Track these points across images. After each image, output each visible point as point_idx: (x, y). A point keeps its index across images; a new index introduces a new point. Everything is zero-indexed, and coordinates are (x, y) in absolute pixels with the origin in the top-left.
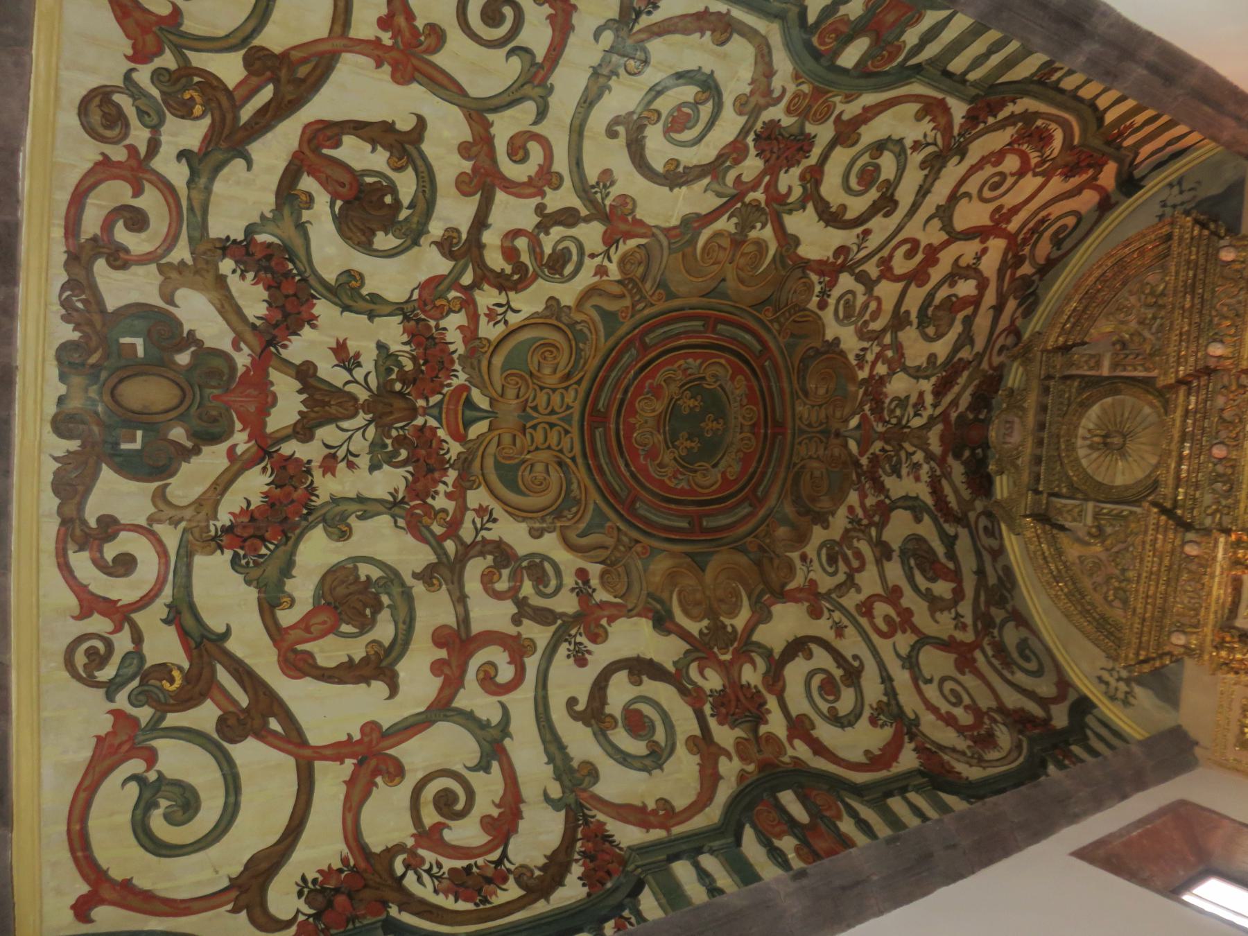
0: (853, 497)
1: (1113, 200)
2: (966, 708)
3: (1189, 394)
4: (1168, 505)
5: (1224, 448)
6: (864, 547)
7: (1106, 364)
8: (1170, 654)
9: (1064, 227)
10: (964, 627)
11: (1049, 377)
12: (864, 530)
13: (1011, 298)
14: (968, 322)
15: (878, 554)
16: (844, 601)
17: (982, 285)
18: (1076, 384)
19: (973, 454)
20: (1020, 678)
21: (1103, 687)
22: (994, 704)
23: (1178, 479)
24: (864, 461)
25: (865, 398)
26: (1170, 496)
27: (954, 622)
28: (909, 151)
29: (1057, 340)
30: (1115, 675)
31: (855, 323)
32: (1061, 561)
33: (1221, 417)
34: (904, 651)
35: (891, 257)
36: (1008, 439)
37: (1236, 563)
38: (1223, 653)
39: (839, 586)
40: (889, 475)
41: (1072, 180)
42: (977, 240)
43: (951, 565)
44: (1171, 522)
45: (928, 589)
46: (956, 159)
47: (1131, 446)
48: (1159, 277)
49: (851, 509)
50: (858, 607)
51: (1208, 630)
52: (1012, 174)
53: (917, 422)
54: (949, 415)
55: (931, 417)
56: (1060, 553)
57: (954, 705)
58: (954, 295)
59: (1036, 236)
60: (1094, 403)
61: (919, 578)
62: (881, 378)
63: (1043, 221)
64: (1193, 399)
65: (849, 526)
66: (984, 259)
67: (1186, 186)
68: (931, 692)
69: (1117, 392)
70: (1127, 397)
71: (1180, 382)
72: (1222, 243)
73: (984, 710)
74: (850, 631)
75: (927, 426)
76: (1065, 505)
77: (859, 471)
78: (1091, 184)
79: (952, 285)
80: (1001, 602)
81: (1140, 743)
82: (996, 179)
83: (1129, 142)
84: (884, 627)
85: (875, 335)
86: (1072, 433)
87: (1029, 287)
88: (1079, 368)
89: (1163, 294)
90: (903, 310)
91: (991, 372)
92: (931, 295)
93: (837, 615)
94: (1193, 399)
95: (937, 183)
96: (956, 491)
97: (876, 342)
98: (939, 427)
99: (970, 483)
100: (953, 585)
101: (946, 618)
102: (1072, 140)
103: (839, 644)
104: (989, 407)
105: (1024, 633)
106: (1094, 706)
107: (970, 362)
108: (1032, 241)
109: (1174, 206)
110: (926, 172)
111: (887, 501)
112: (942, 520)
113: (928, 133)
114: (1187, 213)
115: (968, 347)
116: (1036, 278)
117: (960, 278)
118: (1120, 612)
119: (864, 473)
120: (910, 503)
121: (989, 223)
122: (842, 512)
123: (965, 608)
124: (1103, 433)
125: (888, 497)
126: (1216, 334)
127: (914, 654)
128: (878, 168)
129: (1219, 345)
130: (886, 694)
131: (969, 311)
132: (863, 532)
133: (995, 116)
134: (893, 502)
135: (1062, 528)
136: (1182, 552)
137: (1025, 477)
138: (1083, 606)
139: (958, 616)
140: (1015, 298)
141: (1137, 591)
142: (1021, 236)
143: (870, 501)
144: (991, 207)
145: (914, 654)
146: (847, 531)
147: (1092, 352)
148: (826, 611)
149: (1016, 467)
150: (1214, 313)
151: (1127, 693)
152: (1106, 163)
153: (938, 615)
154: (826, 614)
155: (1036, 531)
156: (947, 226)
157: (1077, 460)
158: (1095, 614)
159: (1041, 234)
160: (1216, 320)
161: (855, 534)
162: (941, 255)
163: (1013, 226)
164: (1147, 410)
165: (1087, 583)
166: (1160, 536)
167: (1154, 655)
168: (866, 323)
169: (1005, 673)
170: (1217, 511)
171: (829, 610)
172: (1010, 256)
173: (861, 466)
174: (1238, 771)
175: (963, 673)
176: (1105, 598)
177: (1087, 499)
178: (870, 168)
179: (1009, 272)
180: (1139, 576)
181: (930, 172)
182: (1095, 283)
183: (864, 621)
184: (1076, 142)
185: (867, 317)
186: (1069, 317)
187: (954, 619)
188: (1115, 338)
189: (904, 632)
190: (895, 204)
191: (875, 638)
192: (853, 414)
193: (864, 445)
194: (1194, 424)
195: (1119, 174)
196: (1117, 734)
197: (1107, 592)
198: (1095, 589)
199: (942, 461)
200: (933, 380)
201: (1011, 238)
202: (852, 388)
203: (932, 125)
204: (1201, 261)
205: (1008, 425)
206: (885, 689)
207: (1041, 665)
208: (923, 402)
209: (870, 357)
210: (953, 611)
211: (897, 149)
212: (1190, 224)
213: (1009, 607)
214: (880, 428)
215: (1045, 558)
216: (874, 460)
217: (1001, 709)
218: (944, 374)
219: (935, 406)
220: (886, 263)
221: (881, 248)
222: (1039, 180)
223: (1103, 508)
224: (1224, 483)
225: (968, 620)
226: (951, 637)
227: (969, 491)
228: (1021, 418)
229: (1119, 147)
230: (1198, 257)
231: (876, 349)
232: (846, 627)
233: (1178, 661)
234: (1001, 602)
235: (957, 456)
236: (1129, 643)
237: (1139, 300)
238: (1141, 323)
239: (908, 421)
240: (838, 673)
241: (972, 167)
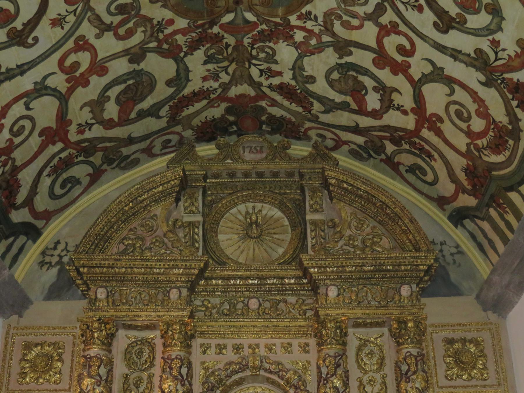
0: (182, 23)
1: (445, 207)
2: (10, 140)
3: (296, 278)
4: (207, 274)
5: (256, 307)
6: (138, 38)
7: (317, 217)
8: (89, 289)
9: (425, 174)
10: (81, 132)
11: (302, 176)
12: (153, 36)
13: (367, 139)
14: (344, 106)
15: (133, 51)
16: (86, 24)
17: (375, 114)
18: (298, 197)
19: (232, 124)
20: (46, 182)
21: (52, 246)
22: (18, 163)
23: (229, 278)
24: (216, 30)
25: (272, 24)
26: (215, 274)
27: (84, 124)
28: (491, 38)
30: (64, 253)
31: (339, 8)
32: (151, 202)
33: (280, 301)
34: (50, 82)
35: (399, 33)
36: (247, 150)
37: (169, 325)
38: (96, 325)
39: (98, 18)
40: (205, 53)
41: (463, 174)
42: (414, 105)
43: (133, 115)
44: (194, 277)
45: (109, 98)
46: (483, 79)
47: (251, 243)
48: (387, 246)
49: (171, 22)
50: (82, 37)
51: (112, 313)
52: (469, 127)
53: (255, 72)
54: (264, 100)
55: (260, 84)
56: (157, 201)
57: (11, 130)
58: (366, 93)
59: (417, 152)
60: (283, 212)
61: (118, 89)
62: (292, 37)
63: (430, 156)
64: (293, 281)
65: (155, 22)
66: (398, 113)
67: (457, 257)
68: (18, 109)
69: (294, 227)
70: (290, 235)
71: (305, 272)
72: (414, 286)
73: (12, 156)
74: (59, 33)
75: (252, 82)
76: (197, 200)
77: (207, 26)
78: (460, 189)
79: (375, 89)
80: (107, 160)
81: (12, 276)
82: (465, 115)
83: (493, 212)
84: (68, 63)
85: (329, 27)
86: (256, 199)
87: (375, 153)
88: (312, 198)
89: (373, 250)
90: (352, 49)
91: (303, 130)
92: (366, 72)
93: (71, 19)
94: (293, 281)
95: (463, 65)
96: (198, 113)
97: (323, 28)
98: (253, 93)
99: (206, 123)
100: (116, 119)
101: (86, 115)
102: (495, 170)
103: (45, 22)
104: (273, 132)
105: (86, 181)
106: (34, 241)
107: (310, 112)
108: (413, 150)
109: (441, 251)
110: (473, 55)
111: (182, 54)
112: (171, 103)
113: (506, 52)
114: (436, 260)
115: (323, 109)
116: (383, 157)
117: (381, 95)
118: (115, 250)
119: (205, 31)
120: (182, 75)
121: (428, 113)
122: (168, 14)
123: (97, 131)
124: (260, 221)
125: (186, 54)
126: (344, 290)
127: (49, 92)
128: (477, 12)
129: (336, 293)
130: (8, 70)
131: (354, 106)
132: (152, 35)
133: (517, 107)
134: (182, 59)
135: (177, 200)
136: (171, 288)
137: (216, 167)
138: (115, 223)
139: (90, 126)
140: (366, 142)
141: (135, 260)
142: (417, 141)
143: (180, 39)
144: (442, 113)
145: (49, 92)
146: (150, 20)
147: (324, 206)
148: (75, 7)
149: (225, 158)
150: (360, 287)
151: (50, 263)
152: (476, 198)
153: (87, 109)
154: (71, 8)
155: (173, 180)
156: (426, 79)
157: (236, 205)
158: (110, 232)
159: (419, 156)
160: (354, 289)
161: (149, 29)
162: (401, 76)
163: (425, 133)
164: (281, 251)
165: (136, 223)
166: (181, 271)
167: (85, 278)
168: (340, 17)
169: (48, 169)
170: (207, 308)
171: (75, 10)
172: (401, 134)
173: (211, 27)
174: (6, 346)
175: (40, 135)
176: (125, 238)
177: (203, 215)
178: (477, 4)
179: (388, 135)
180: (148, 260)
181: (473, 58)
182: (381, 201)
183: (70, 44)
184: (493, 173)
185: (345, 18)
186: (352, 185)
187: (86, 123)
188: (337, 221)
189: (68, 81)
190: (446, 32)
191: (57, 55)
192: (257, 15)
193: (229, 28)
194: (273, 284)
195: (467, 208)
196: (15, 259)
197: (130, 239)
198: (131, 230)
199: (222, 98)
200: (293, 83)
201: (416, 132)
202: (280, 11)
203: (513, 54)
204: (400, 274)
205: (258, 149)
206: (12, 69)
207: (61, 196)
208: (273, 77)
209: (309, 25)
210: (93, 121)
211: (493, 27)
212: (428, 262)
213: (105, 167)
214: (247, 41)
215: (151, 189)
216: (218, 38)
217: (16, 170)
218: (299, 91)
219: (270, 87)
220: (393, 29)
221: (406, 23)
222: (463, 149)
223: (198, 228)
224: (229, 310)
225: (88, 135)
226: (70, 122)
227: (200, 124)
228: (266, 158)
229: (489, 206)
230: (403, 271)
231: (316, 30)
232: (62, 28)
233: (84, 296)
234: (107, 160)
235: (228, 111)
236: (92, 259)
237: (368, 235)
238: (350, 238)
239: (255, 65)
240: (18, 24)
241: (476, 93)
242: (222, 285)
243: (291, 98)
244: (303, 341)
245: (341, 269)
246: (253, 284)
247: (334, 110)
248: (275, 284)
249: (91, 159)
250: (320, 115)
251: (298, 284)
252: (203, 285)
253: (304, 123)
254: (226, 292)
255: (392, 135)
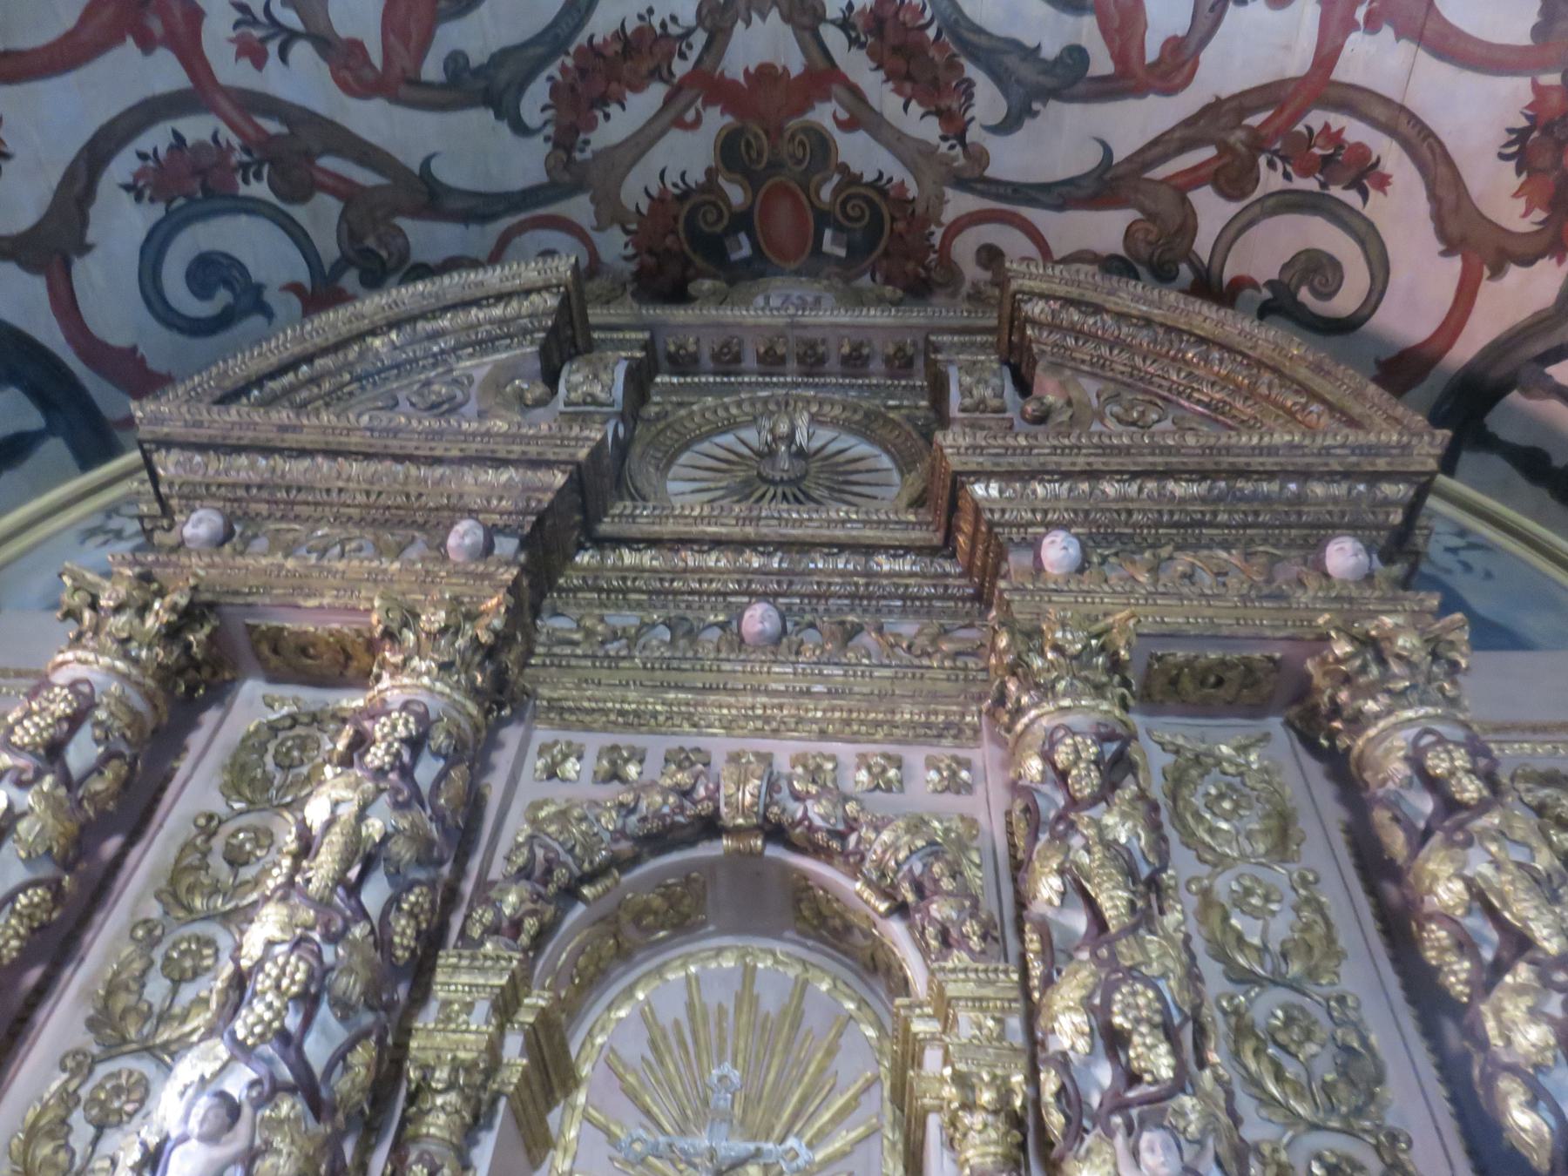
29: (1033, 295)
54: (827, 98)
64: (905, 565)
107: (961, 137)
112: (553, 70)
150: (1164, 552)
172: (1255, 120)
194: (835, 572)
218: (931, 33)
230: (1322, 503)
235: (730, 150)
242: (654, 570)
243: (908, 77)
244: (945, 750)
245: (1084, 486)
246: (763, 572)
247: (1036, 106)
248: (842, 574)
249: (299, 213)
250: (993, 144)
251: (923, 575)
252: (587, 568)
253: (942, 201)
254: (666, 593)
255: (1224, 148)
